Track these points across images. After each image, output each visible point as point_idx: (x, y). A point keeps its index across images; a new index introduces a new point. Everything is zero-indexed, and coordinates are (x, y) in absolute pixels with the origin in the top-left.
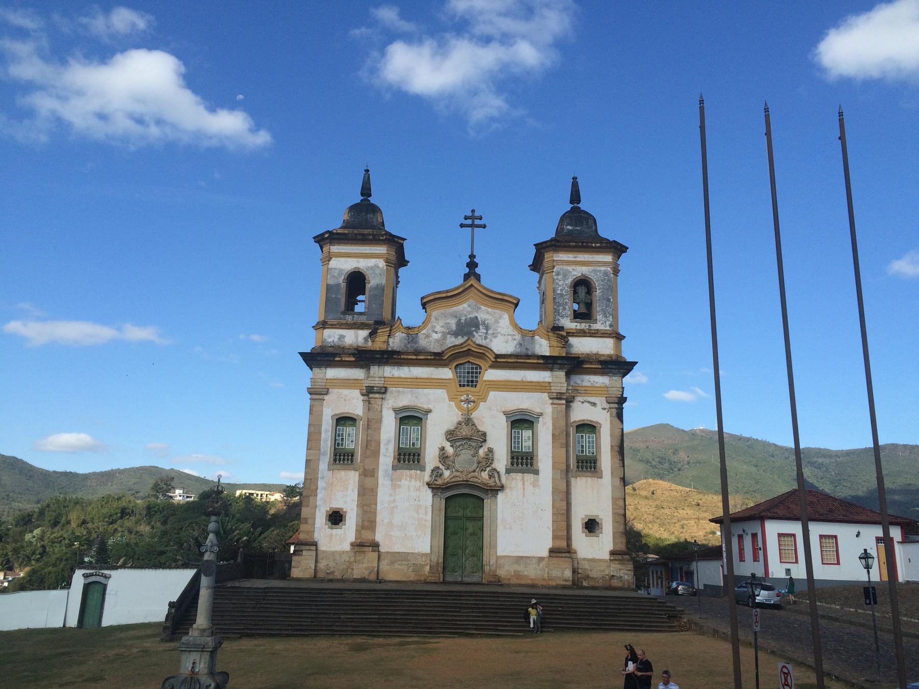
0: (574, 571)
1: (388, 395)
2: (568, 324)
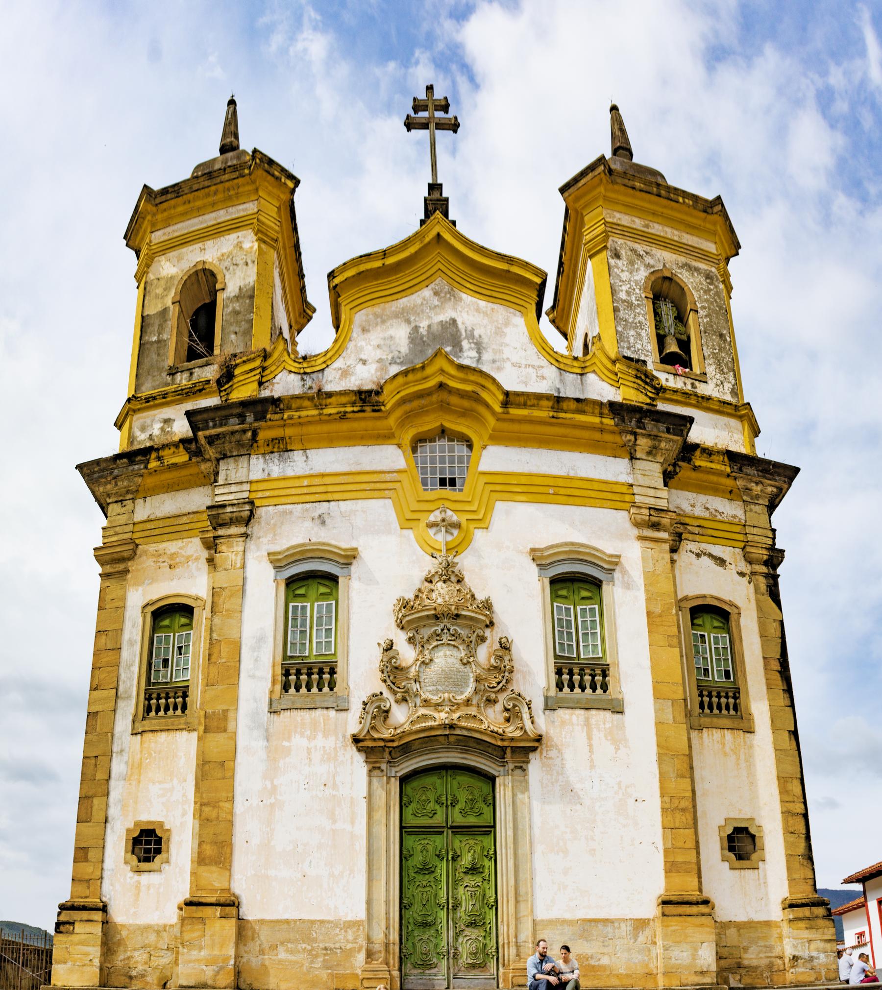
1: (255, 529)
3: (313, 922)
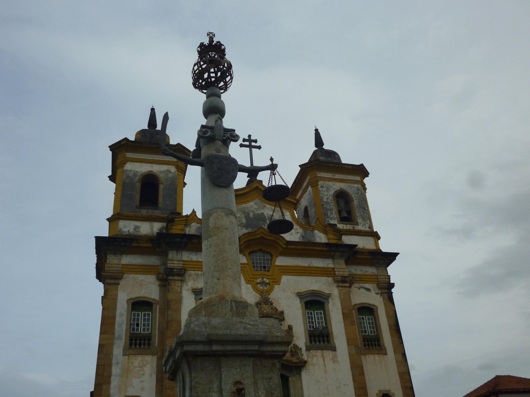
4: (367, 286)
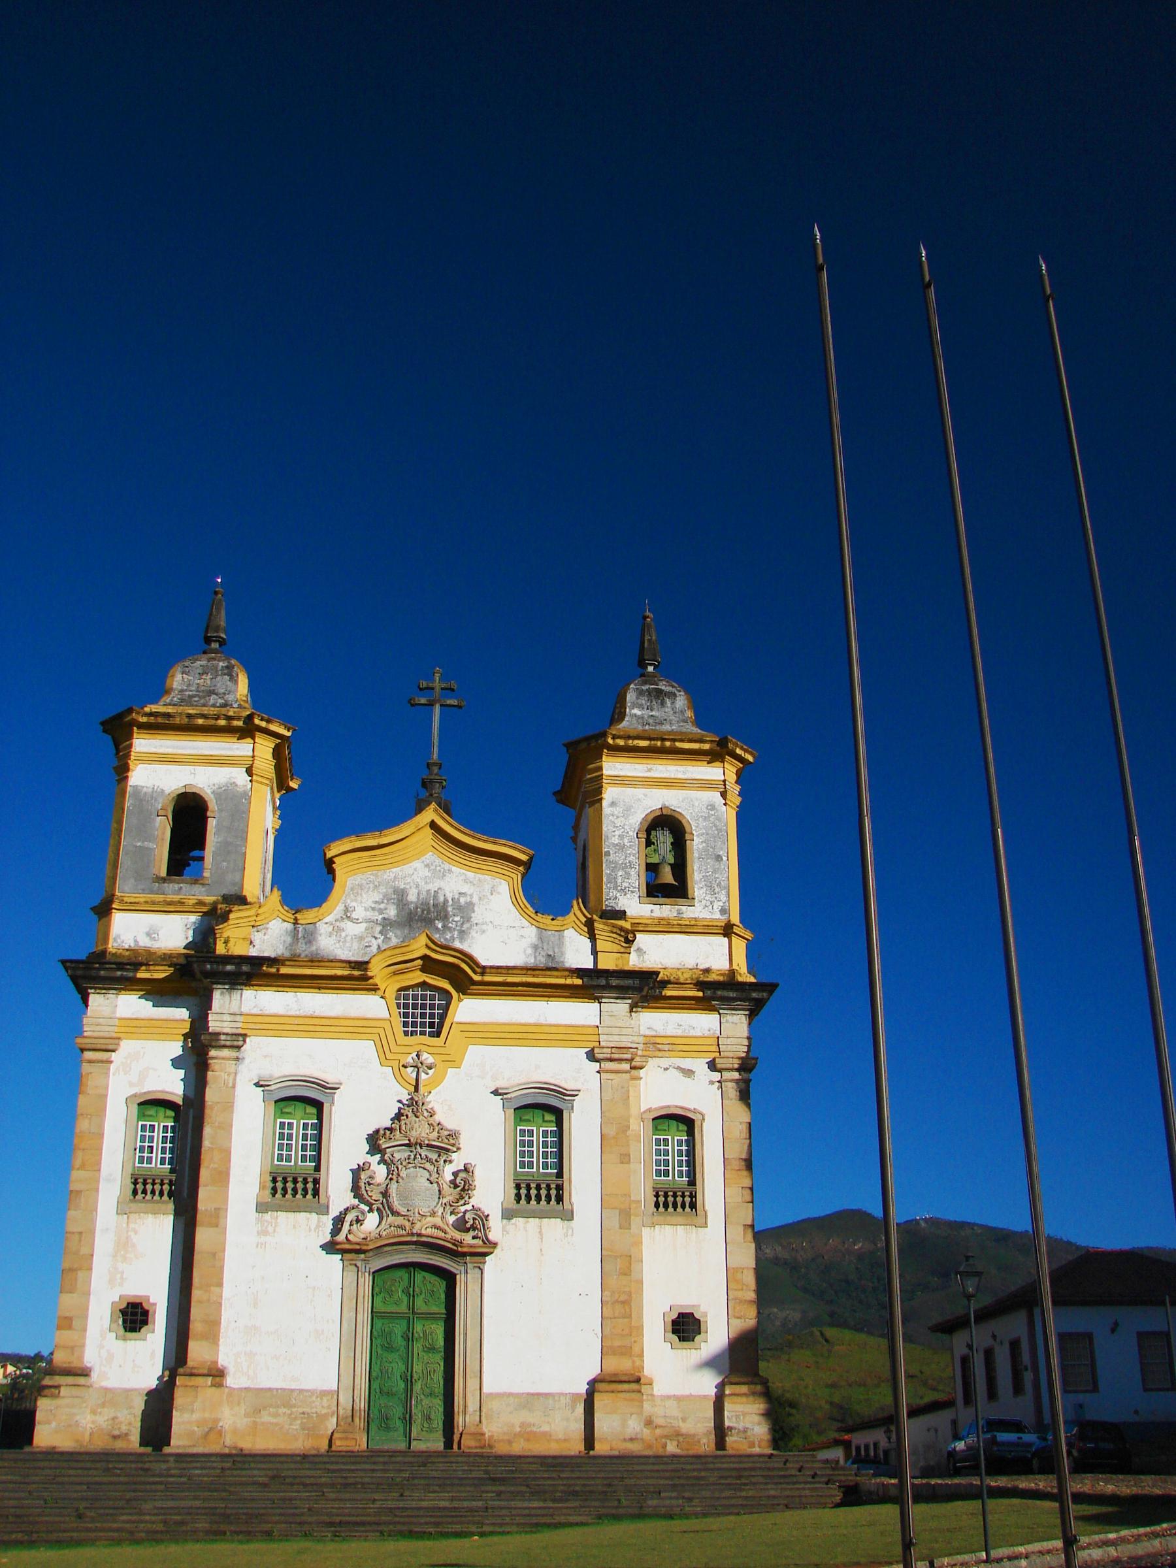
0: (649, 1423)
2: (636, 906)
3: (292, 1390)
4: (687, 1063)
